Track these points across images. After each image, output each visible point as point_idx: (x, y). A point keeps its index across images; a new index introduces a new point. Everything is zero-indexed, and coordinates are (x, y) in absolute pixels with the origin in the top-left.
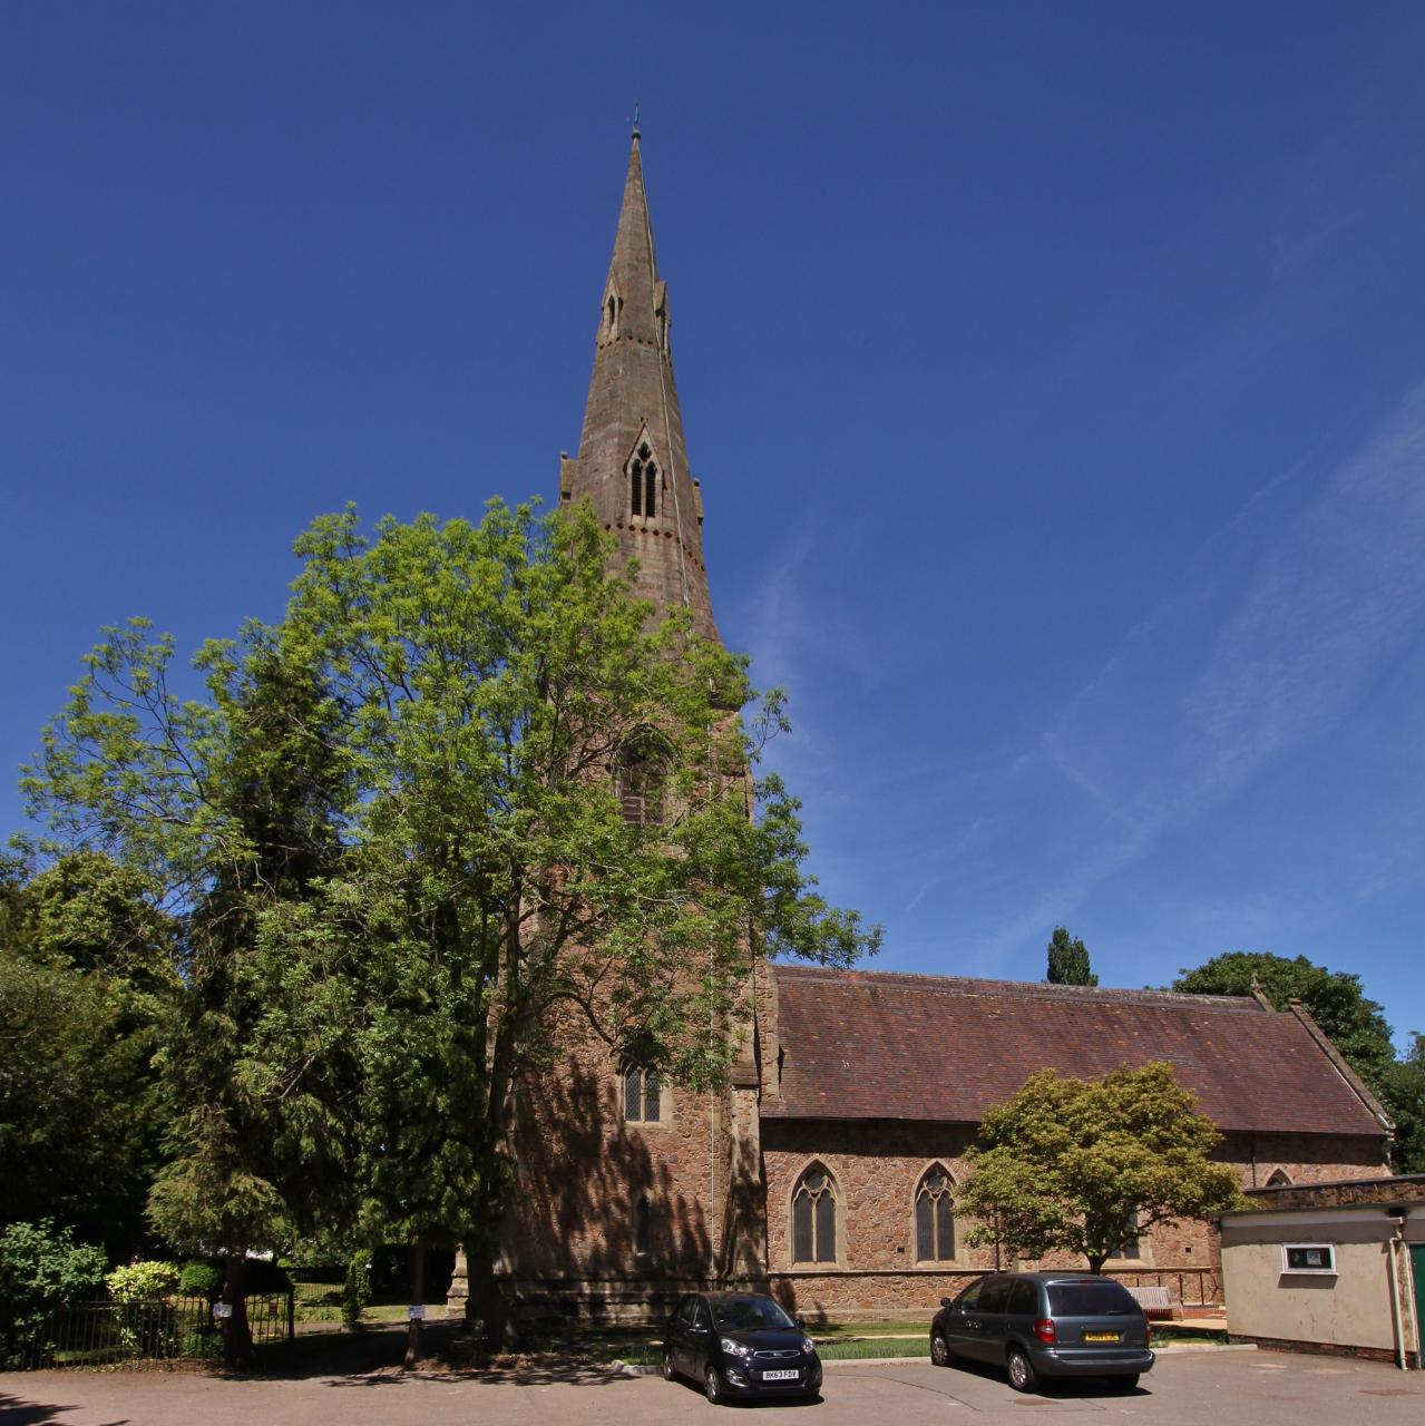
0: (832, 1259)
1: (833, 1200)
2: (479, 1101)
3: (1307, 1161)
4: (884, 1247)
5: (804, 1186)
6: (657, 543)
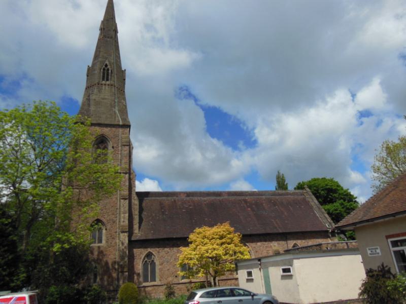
0: (155, 281)
1: (155, 263)
2: (62, 253)
3: (304, 239)
4: (171, 276)
5: (146, 259)
6: (108, 88)
